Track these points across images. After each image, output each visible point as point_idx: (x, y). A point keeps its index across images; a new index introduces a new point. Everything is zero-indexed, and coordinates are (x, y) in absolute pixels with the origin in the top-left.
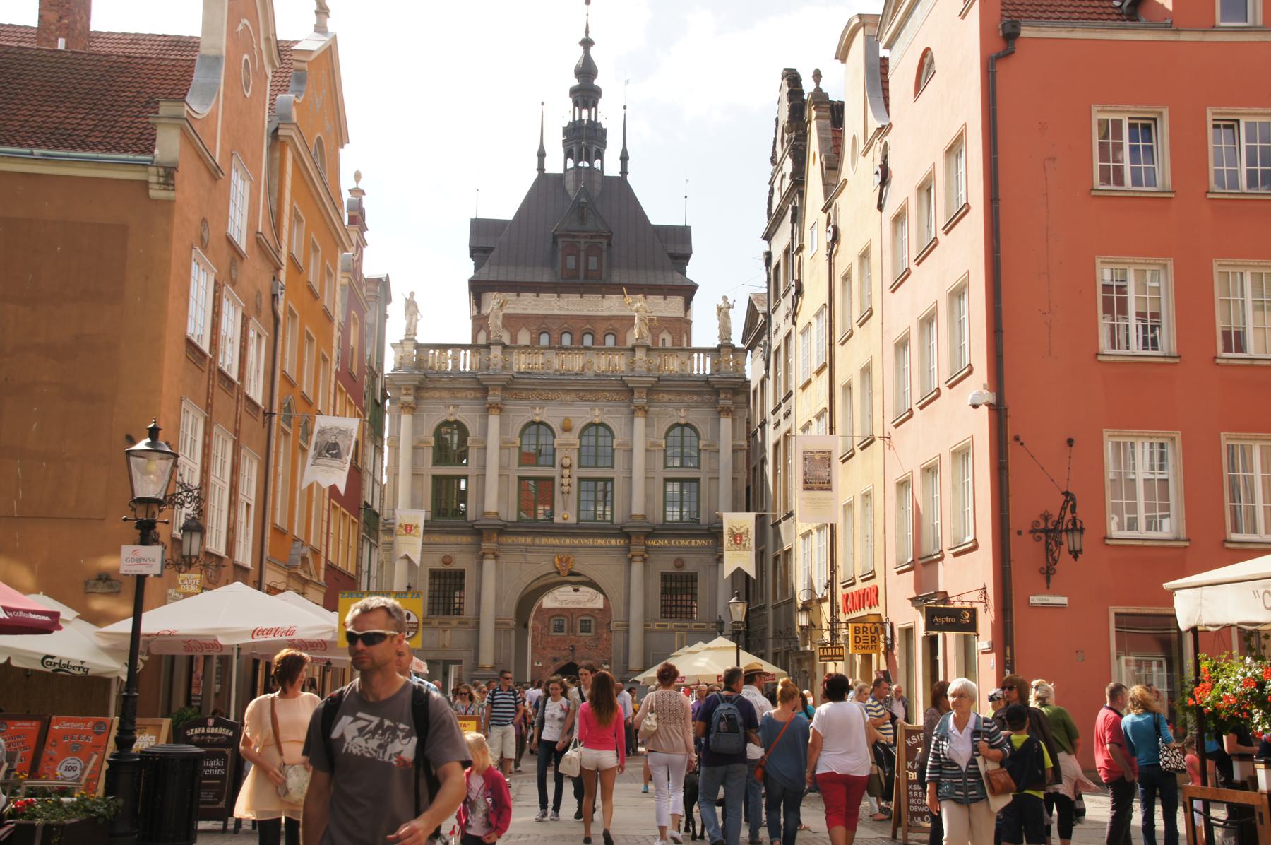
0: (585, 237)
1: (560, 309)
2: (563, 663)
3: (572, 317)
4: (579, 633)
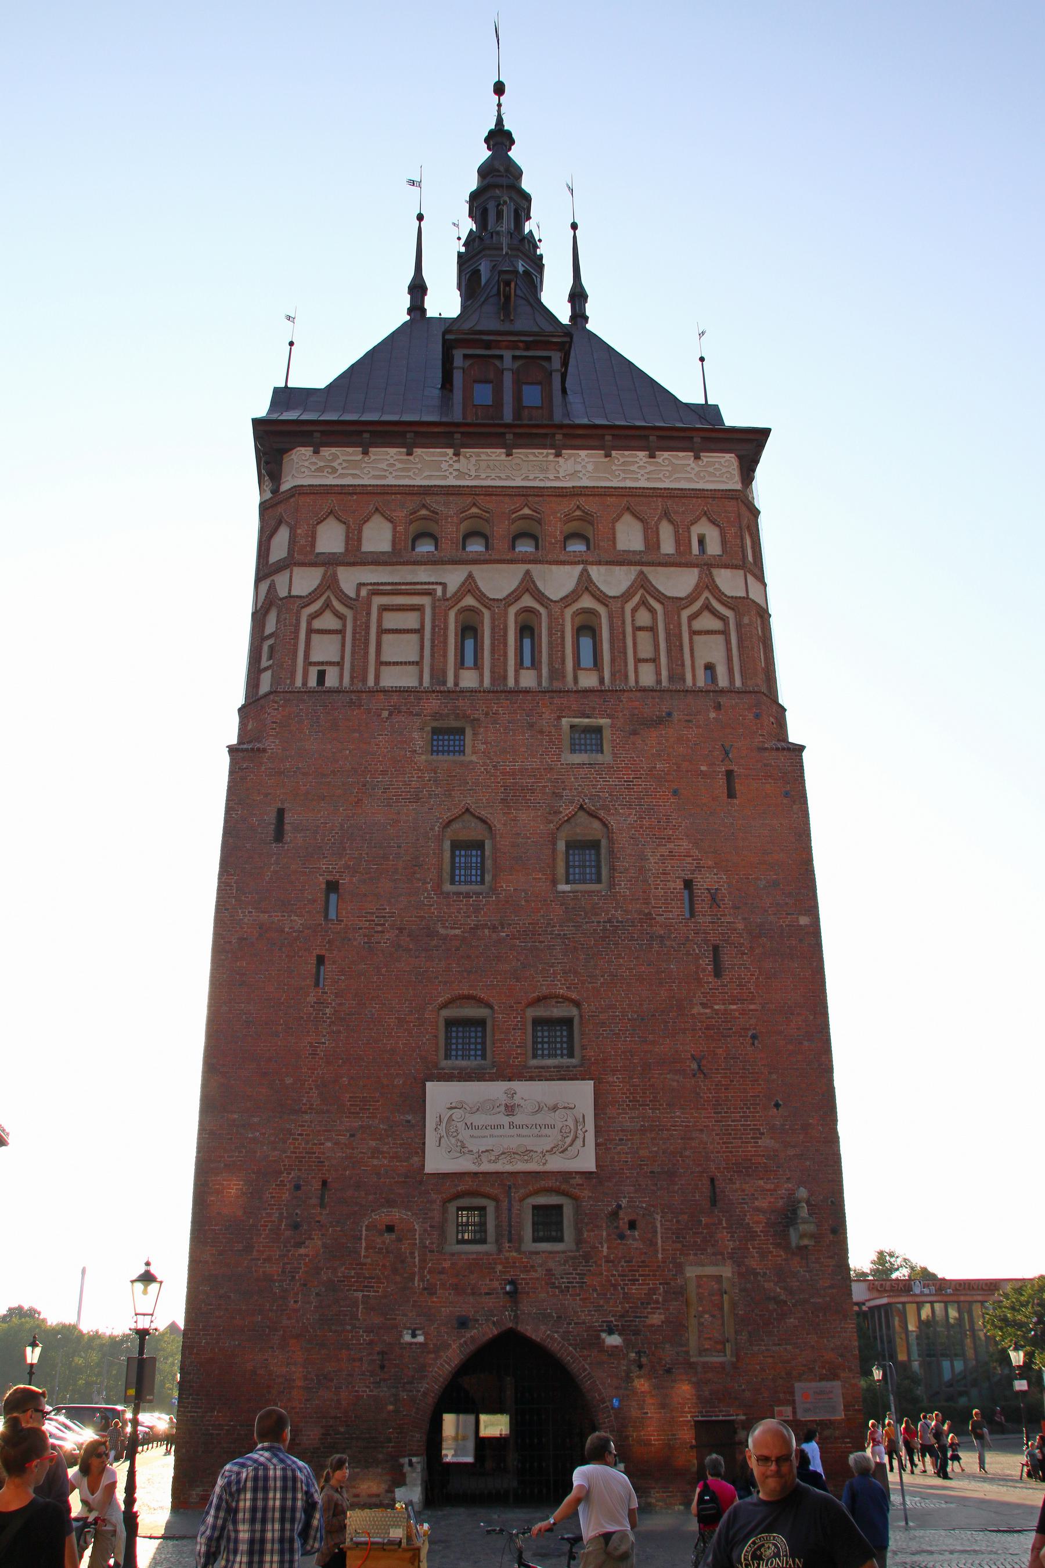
0: (513, 346)
1: (461, 475)
2: (485, 1331)
3: (489, 492)
4: (529, 1245)
